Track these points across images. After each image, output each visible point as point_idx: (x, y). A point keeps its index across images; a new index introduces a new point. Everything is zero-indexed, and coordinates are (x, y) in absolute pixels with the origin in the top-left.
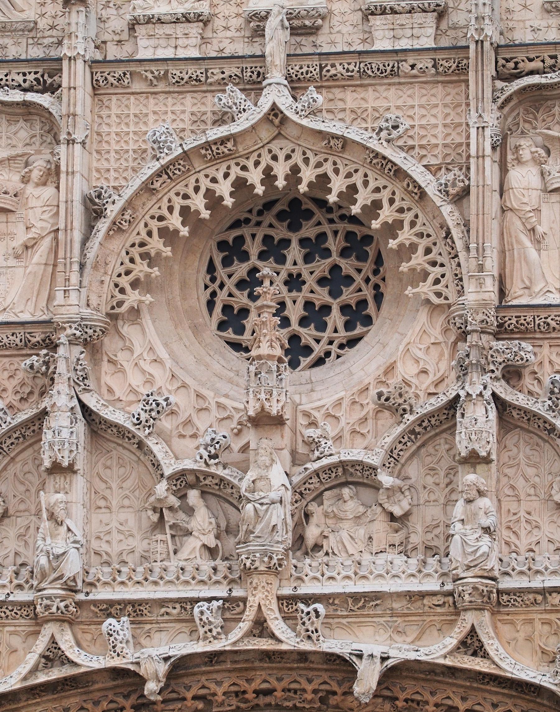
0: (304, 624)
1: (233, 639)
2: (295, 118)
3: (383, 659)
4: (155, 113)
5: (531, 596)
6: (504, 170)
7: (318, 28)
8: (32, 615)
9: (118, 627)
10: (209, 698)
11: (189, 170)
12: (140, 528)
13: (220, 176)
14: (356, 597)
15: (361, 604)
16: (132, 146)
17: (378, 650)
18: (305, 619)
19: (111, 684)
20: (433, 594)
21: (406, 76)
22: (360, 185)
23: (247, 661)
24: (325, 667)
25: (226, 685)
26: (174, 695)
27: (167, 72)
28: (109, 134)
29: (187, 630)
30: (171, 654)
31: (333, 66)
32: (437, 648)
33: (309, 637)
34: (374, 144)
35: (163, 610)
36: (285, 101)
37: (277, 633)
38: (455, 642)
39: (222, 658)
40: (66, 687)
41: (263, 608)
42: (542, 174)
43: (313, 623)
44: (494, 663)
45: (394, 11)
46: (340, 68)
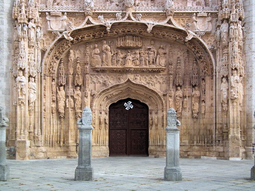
0: (137, 17)
1: (125, 20)
3: (153, 24)
5: (180, 14)
8: (84, 15)
9: (101, 17)
10: (118, 32)
12: (103, 1)
14: (147, 13)
15: (148, 15)
17: (152, 23)
18: (138, 16)
19: (99, 29)
20: (162, 13)
23: (126, 25)
24: (141, 26)
25: (121, 29)
26: (111, 31)
29: (114, 19)
30: (112, 22)
32: (164, 23)
33: (139, 20)
35: (109, 15)
37: (133, 20)
38: (167, 22)
39: (121, 24)
40: (91, 29)
41: (130, 14)
43: (139, 17)
44: (174, 25)
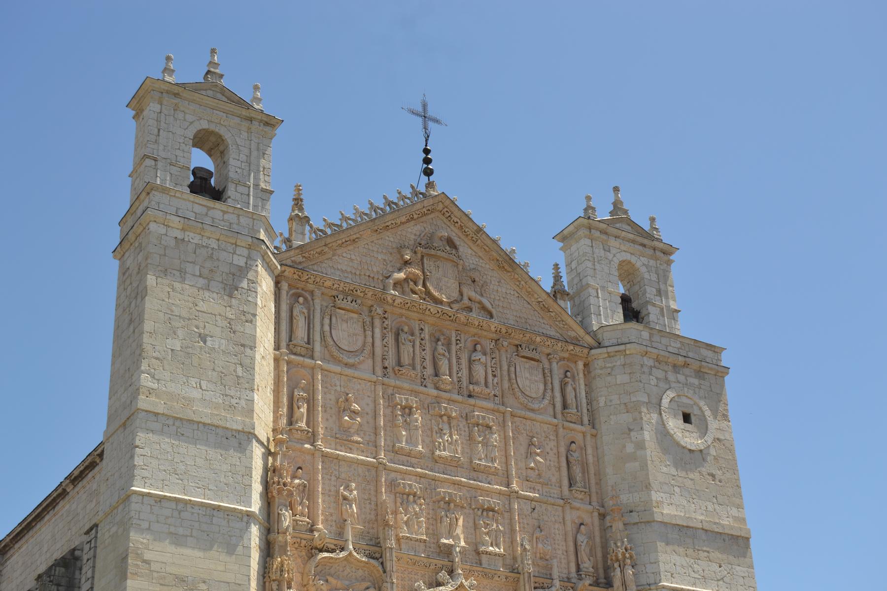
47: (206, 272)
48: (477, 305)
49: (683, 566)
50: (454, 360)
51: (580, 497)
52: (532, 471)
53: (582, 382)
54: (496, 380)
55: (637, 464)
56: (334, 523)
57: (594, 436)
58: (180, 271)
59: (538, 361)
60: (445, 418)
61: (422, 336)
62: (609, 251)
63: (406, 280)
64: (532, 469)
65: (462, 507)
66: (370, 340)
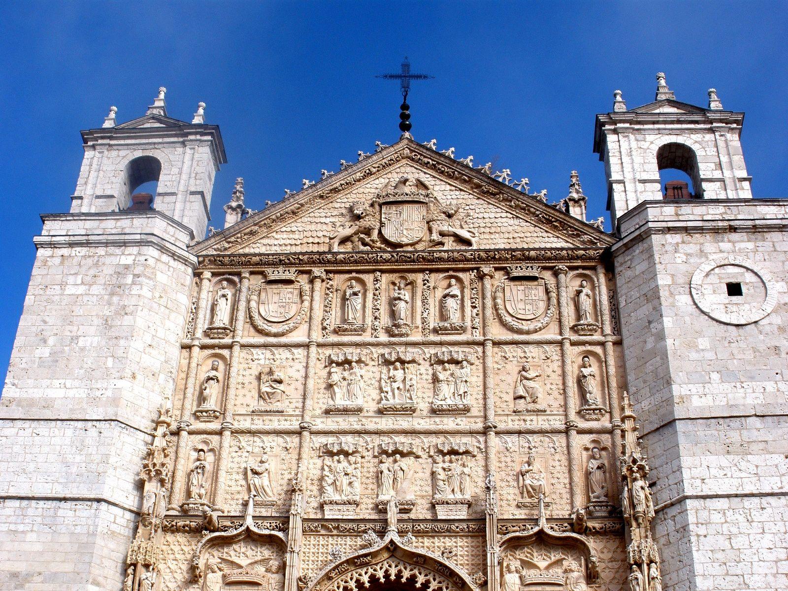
2: (401, 546)
4: (332, 544)
6: (502, 575)
7: (411, 510)
11: (348, 569)
13: (363, 573)
16: (321, 559)
21: (454, 532)
22: (432, 580)
27: (339, 525)
28: (309, 553)
31: (419, 525)
34: (440, 559)
36: (397, 540)
42: (521, 578)
45: (447, 503)
46: (422, 527)
47: (88, 279)
48: (452, 238)
49: (721, 468)
50: (419, 303)
51: (594, 417)
52: (523, 400)
53: (604, 289)
54: (475, 311)
55: (658, 358)
56: (241, 502)
57: (618, 343)
58: (61, 285)
59: (534, 279)
60: (398, 364)
61: (377, 286)
62: (645, 141)
63: (356, 233)
64: (521, 397)
65: (418, 457)
66: (306, 304)
